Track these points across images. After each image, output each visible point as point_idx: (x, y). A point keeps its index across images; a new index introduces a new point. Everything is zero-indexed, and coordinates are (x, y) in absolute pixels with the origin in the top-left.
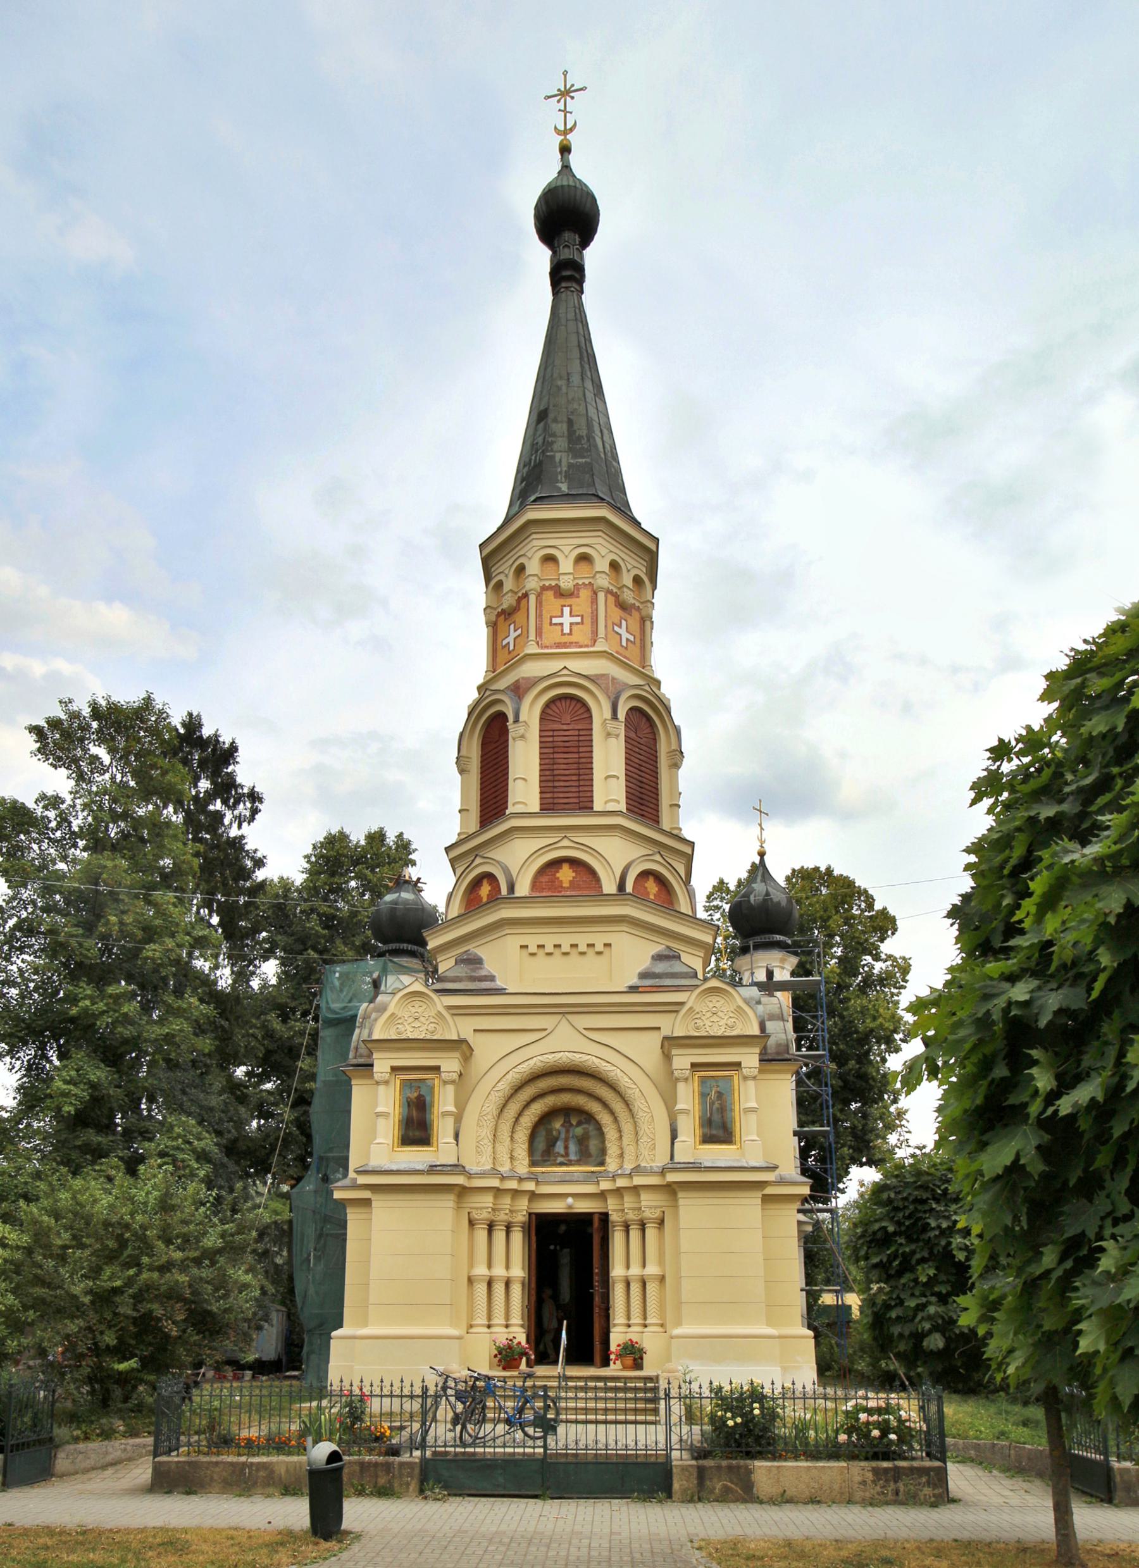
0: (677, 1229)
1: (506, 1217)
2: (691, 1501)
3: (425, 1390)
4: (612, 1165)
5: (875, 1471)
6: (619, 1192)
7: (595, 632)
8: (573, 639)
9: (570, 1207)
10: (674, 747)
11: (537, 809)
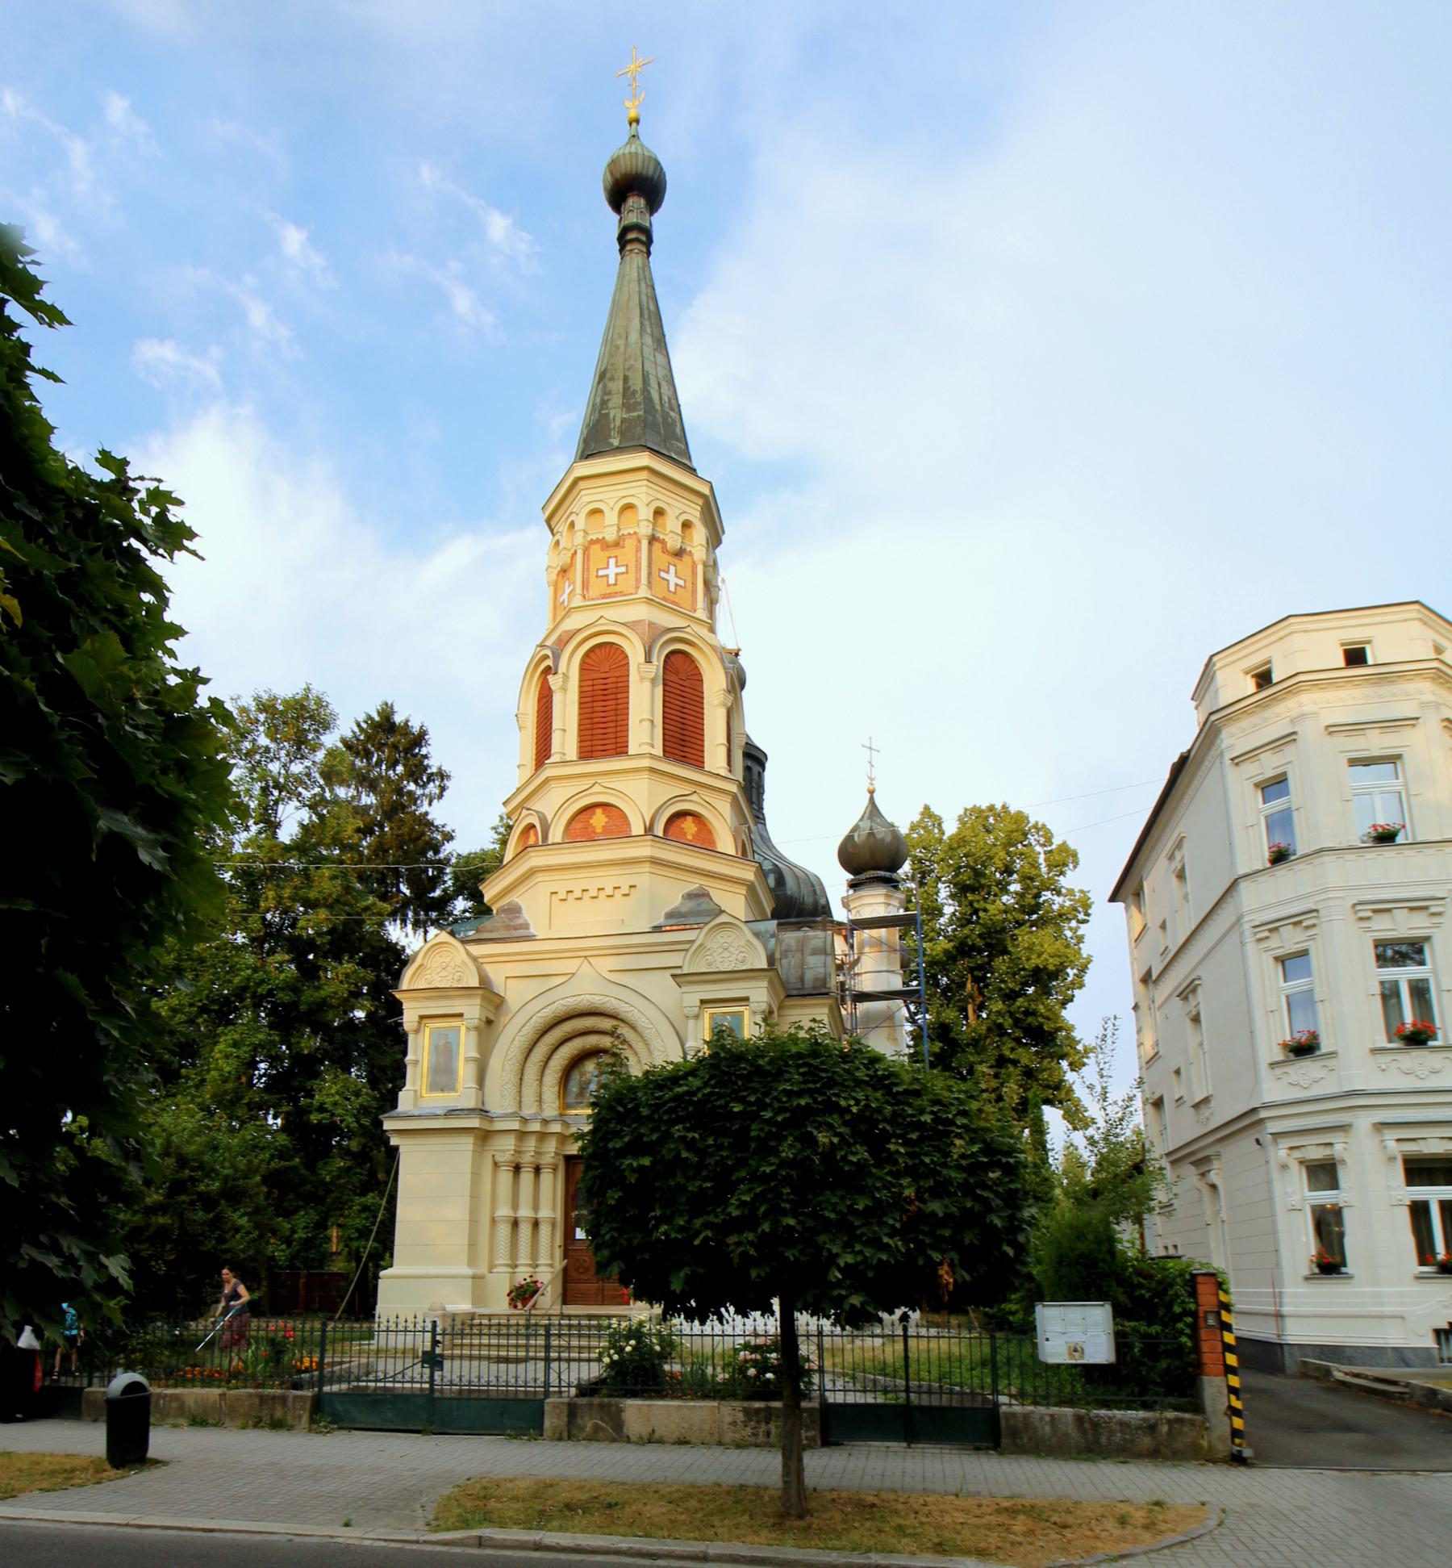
2: (560, 1439)
3: (434, 1323)
5: (746, 1411)
7: (638, 580)
8: (617, 589)
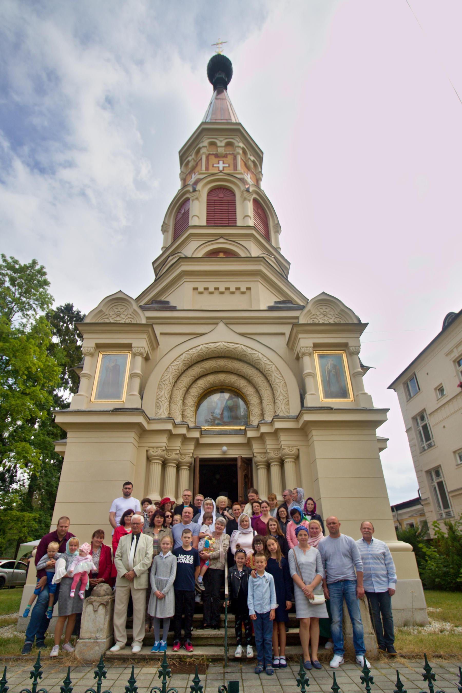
0: (312, 462)
1: (177, 457)
4: (255, 421)
6: (262, 438)
9: (224, 453)
10: (276, 222)
11: (205, 224)
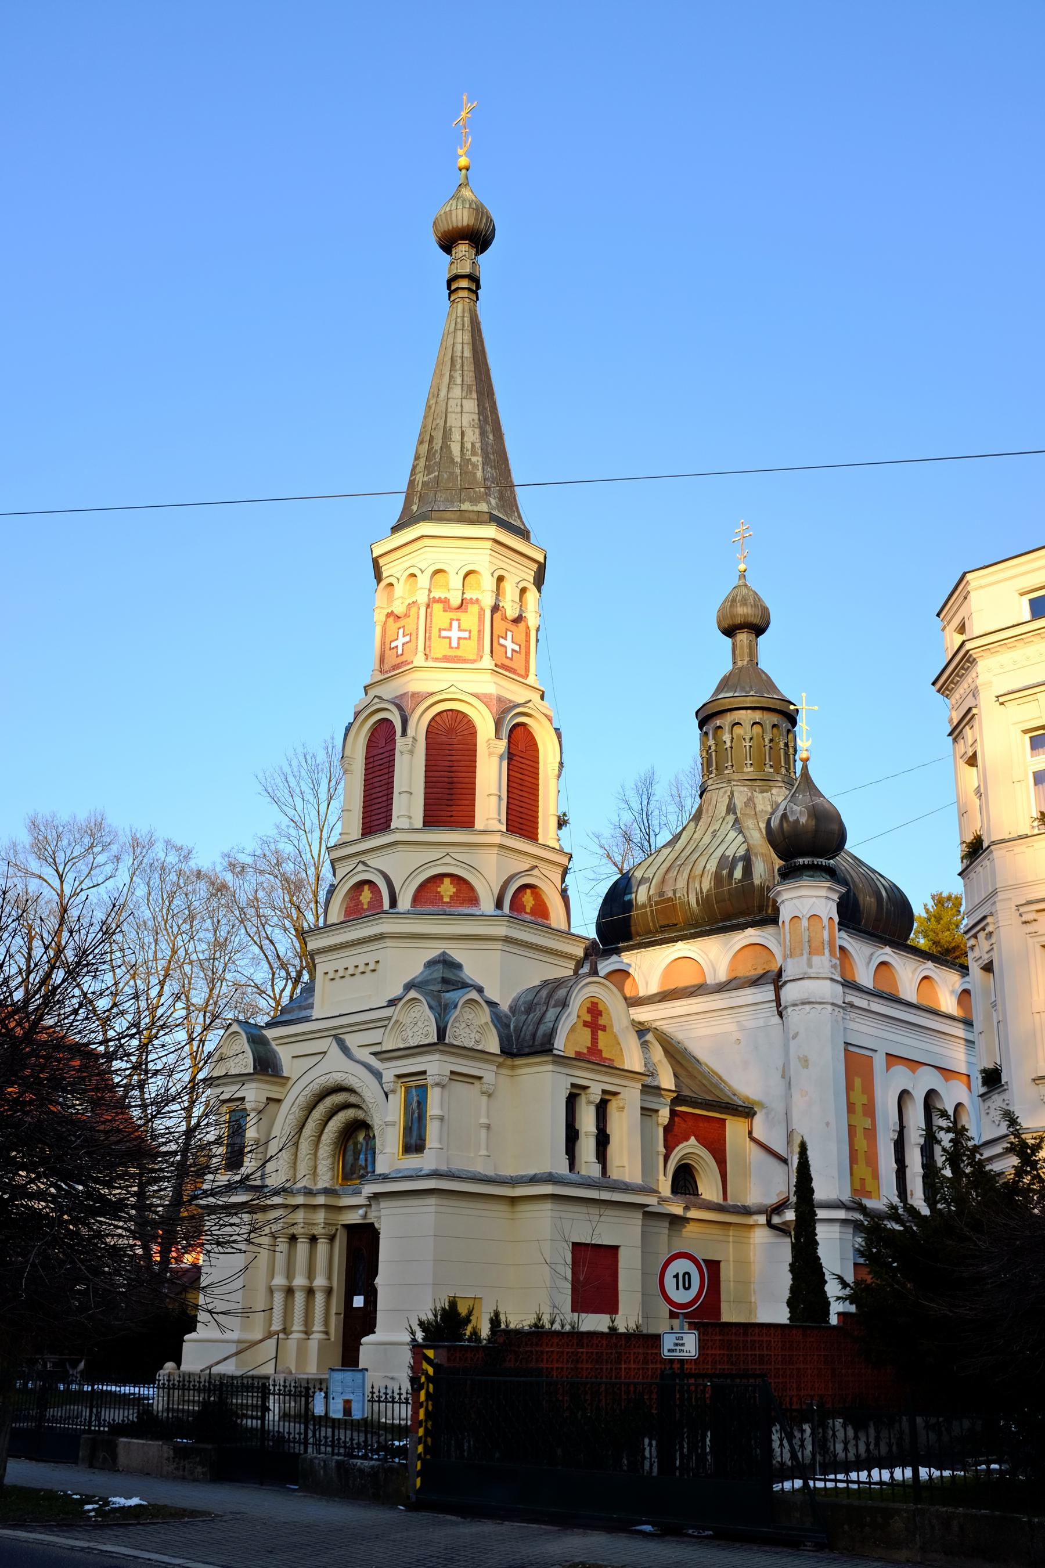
8: (458, 653)
